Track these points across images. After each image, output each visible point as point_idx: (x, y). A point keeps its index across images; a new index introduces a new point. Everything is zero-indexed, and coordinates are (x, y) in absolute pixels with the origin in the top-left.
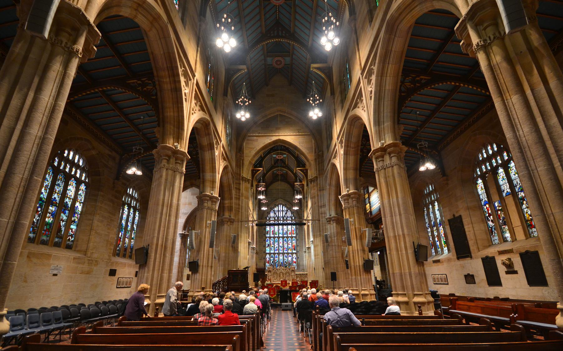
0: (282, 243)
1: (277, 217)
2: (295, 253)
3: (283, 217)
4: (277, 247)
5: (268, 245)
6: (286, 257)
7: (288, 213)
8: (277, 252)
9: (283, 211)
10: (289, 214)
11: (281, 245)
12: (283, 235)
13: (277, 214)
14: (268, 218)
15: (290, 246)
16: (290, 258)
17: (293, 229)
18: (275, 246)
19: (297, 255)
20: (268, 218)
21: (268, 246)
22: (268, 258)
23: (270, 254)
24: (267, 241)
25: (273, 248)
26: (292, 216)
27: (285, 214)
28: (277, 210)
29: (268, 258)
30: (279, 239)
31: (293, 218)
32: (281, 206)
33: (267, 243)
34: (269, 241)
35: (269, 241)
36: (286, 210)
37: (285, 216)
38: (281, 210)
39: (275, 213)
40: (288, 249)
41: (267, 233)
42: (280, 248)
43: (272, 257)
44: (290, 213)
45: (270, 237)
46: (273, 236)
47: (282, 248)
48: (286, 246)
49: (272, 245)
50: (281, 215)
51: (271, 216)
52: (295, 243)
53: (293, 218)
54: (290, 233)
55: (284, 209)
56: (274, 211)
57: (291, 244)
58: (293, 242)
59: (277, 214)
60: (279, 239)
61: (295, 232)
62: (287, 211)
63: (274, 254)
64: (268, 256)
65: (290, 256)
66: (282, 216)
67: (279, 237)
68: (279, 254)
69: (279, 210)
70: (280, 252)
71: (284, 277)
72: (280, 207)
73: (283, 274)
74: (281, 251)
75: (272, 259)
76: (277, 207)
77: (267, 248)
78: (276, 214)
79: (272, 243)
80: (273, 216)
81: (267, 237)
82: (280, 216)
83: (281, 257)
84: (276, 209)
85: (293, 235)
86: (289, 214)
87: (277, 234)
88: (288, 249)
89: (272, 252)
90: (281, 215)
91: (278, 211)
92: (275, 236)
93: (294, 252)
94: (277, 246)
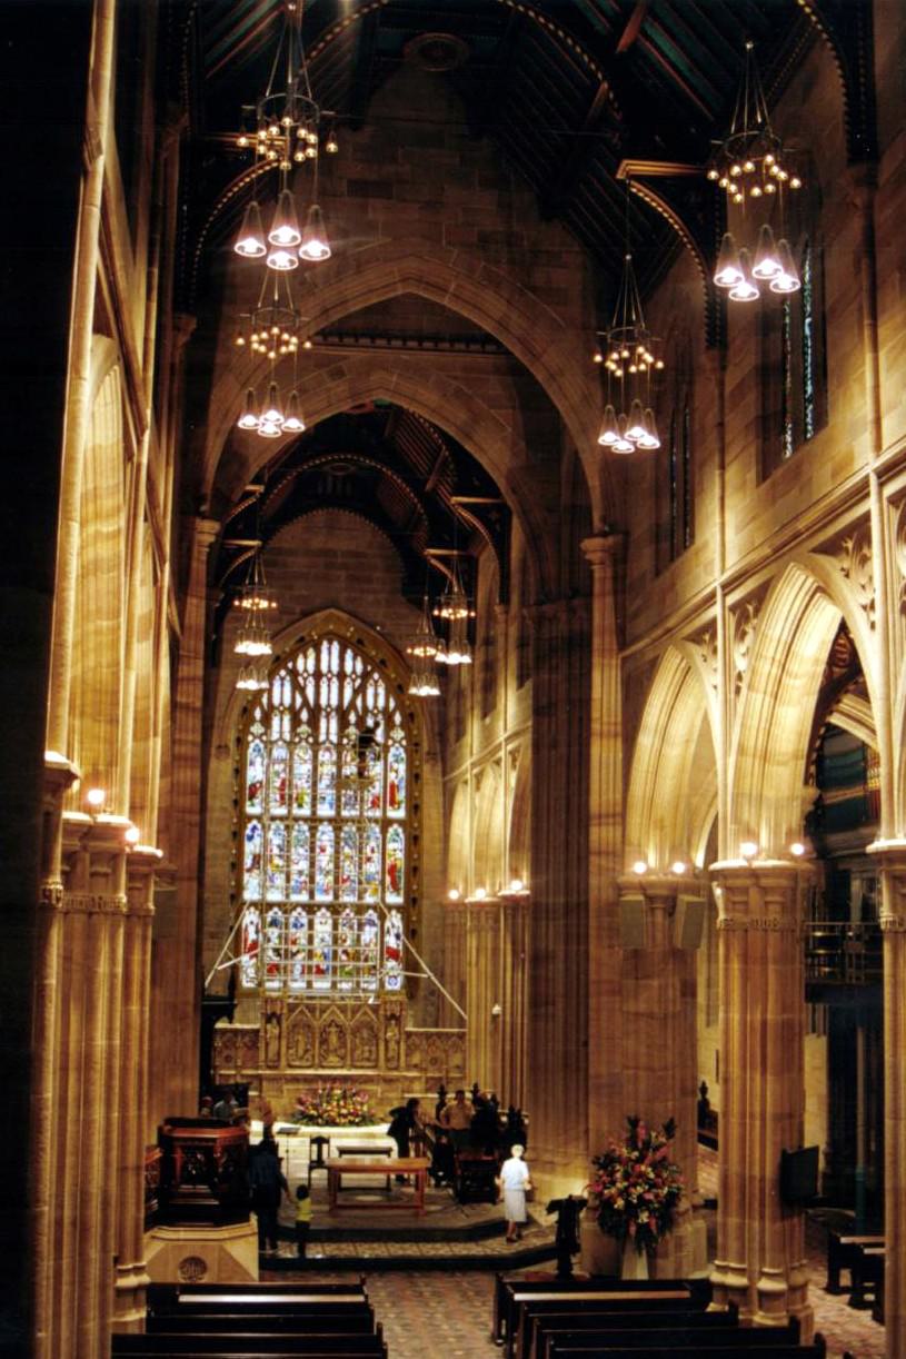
0: (330, 850)
1: (310, 711)
2: (399, 908)
3: (342, 715)
4: (300, 873)
5: (256, 859)
6: (351, 928)
7: (370, 691)
8: (304, 897)
9: (342, 676)
10: (376, 695)
11: (324, 860)
12: (338, 813)
13: (310, 692)
14: (258, 714)
15: (373, 868)
16: (369, 934)
17: (392, 776)
18: (294, 868)
19: (406, 921)
20: (258, 714)
21: (253, 867)
22: (252, 929)
23: (263, 907)
24: (251, 838)
25: (280, 880)
26: (392, 704)
27: (356, 692)
28: (311, 668)
29: (252, 929)
30: (313, 830)
31: (398, 718)
32: (336, 647)
33: (251, 848)
34: (257, 840)
35: (257, 840)
36: (359, 668)
37: (352, 704)
38: (335, 669)
39: (298, 688)
40: (362, 884)
41: (252, 796)
42: (319, 878)
43: (274, 923)
44: (381, 691)
45: (265, 819)
46: (282, 811)
47: (331, 878)
48: (349, 869)
49: (277, 861)
50: (329, 695)
51: (276, 701)
52: (400, 855)
53: (398, 718)
54: (375, 804)
55: (348, 669)
56: (294, 673)
57: (377, 857)
58: (390, 846)
59: (310, 692)
60: (313, 830)
61: (401, 795)
62: (366, 676)
63: (286, 908)
64: (250, 918)
65: (372, 923)
66: (334, 702)
67: (314, 821)
68: (311, 909)
69: (324, 668)
70: (320, 898)
71: (344, 1045)
72: (330, 656)
73: (341, 1032)
74: (326, 892)
75: (273, 933)
76: (311, 653)
77: (246, 876)
78: (302, 690)
79: (276, 851)
80: (287, 701)
81: (250, 818)
82: (323, 702)
83: (323, 927)
84: (305, 663)
85: (393, 814)
86: (376, 695)
87: (307, 799)
88: (362, 884)
89: (274, 896)
90: (329, 695)
91: (318, 675)
92: (296, 811)
93: (394, 899)
94: (304, 865)
